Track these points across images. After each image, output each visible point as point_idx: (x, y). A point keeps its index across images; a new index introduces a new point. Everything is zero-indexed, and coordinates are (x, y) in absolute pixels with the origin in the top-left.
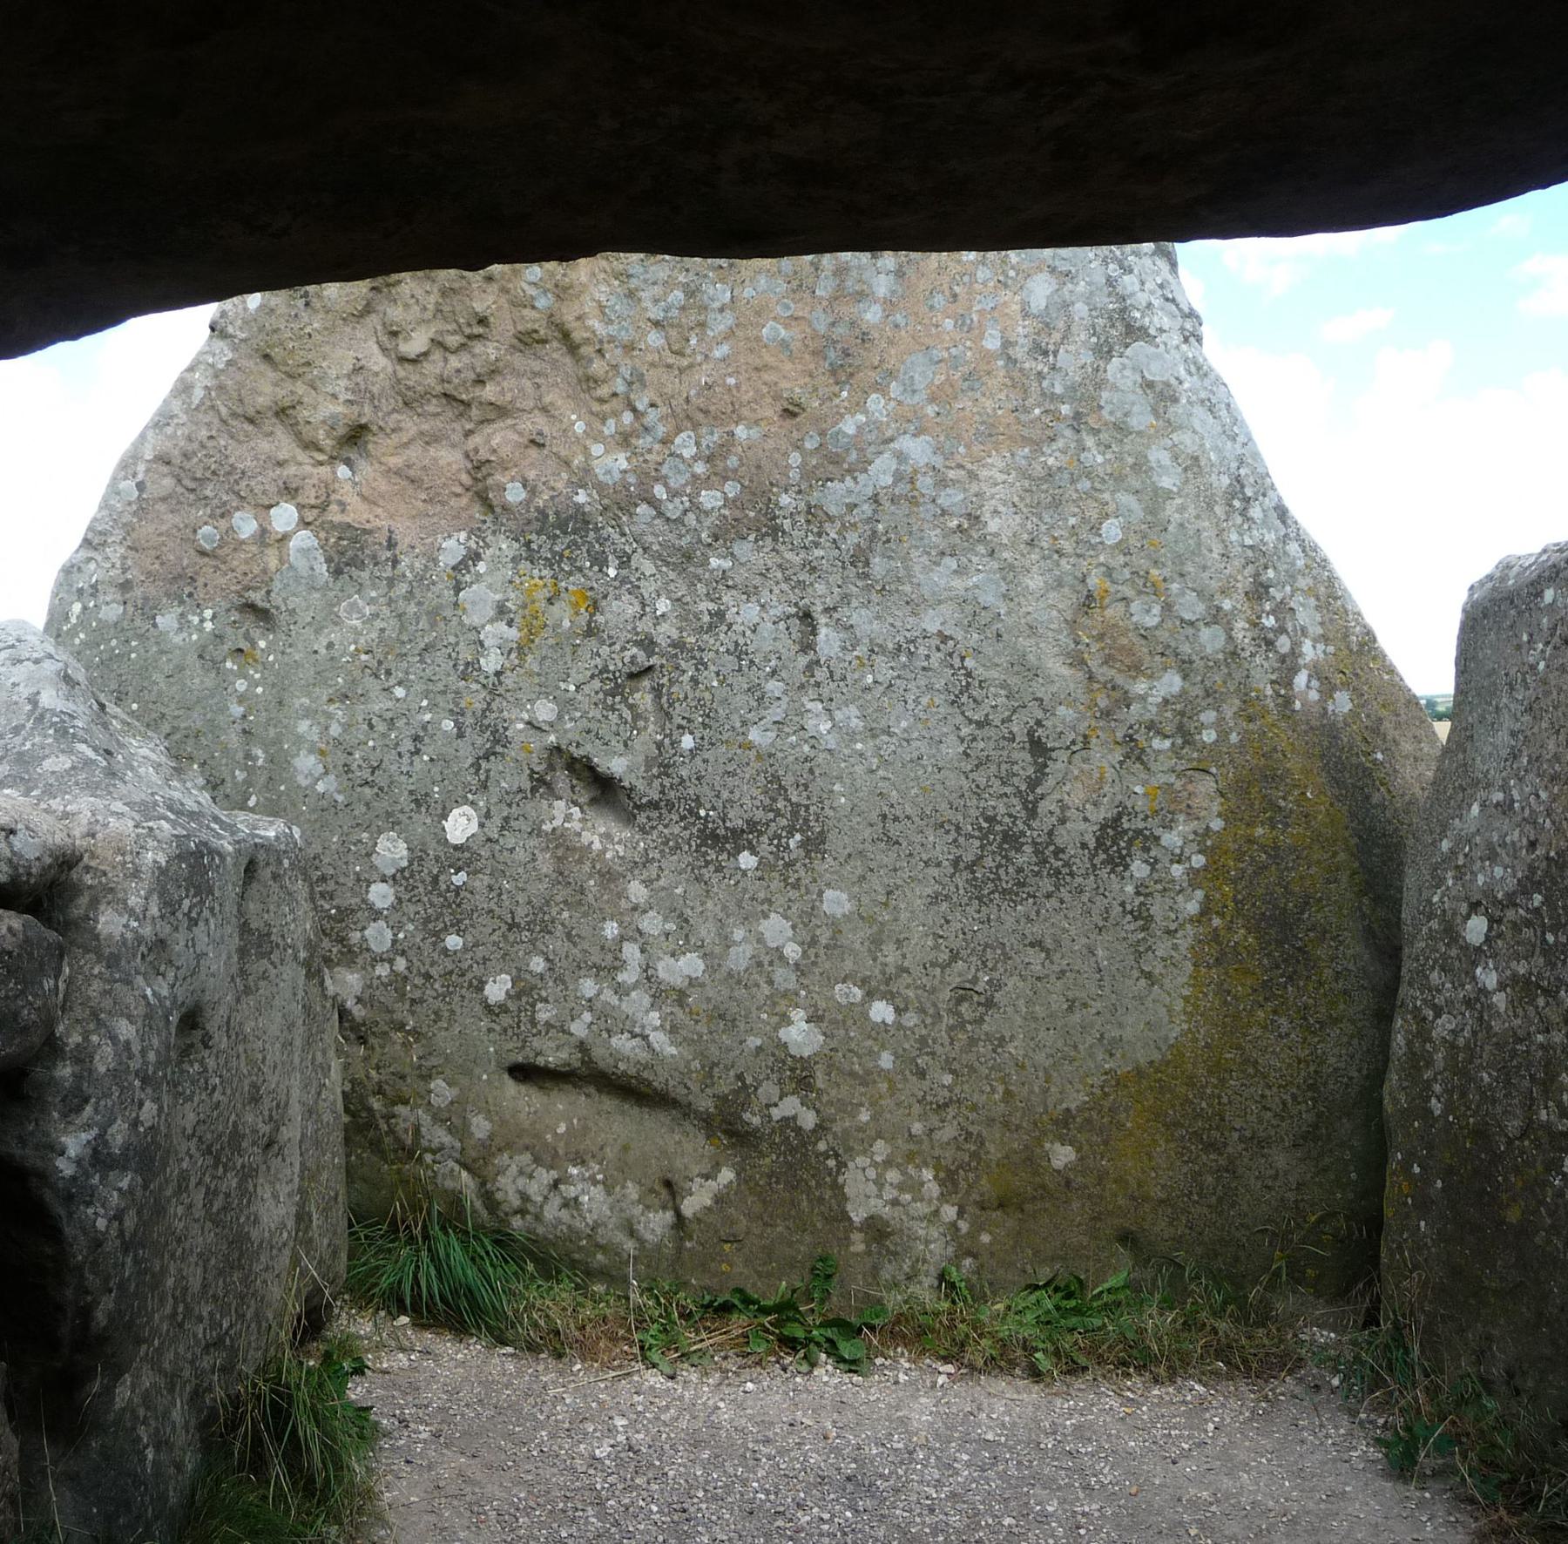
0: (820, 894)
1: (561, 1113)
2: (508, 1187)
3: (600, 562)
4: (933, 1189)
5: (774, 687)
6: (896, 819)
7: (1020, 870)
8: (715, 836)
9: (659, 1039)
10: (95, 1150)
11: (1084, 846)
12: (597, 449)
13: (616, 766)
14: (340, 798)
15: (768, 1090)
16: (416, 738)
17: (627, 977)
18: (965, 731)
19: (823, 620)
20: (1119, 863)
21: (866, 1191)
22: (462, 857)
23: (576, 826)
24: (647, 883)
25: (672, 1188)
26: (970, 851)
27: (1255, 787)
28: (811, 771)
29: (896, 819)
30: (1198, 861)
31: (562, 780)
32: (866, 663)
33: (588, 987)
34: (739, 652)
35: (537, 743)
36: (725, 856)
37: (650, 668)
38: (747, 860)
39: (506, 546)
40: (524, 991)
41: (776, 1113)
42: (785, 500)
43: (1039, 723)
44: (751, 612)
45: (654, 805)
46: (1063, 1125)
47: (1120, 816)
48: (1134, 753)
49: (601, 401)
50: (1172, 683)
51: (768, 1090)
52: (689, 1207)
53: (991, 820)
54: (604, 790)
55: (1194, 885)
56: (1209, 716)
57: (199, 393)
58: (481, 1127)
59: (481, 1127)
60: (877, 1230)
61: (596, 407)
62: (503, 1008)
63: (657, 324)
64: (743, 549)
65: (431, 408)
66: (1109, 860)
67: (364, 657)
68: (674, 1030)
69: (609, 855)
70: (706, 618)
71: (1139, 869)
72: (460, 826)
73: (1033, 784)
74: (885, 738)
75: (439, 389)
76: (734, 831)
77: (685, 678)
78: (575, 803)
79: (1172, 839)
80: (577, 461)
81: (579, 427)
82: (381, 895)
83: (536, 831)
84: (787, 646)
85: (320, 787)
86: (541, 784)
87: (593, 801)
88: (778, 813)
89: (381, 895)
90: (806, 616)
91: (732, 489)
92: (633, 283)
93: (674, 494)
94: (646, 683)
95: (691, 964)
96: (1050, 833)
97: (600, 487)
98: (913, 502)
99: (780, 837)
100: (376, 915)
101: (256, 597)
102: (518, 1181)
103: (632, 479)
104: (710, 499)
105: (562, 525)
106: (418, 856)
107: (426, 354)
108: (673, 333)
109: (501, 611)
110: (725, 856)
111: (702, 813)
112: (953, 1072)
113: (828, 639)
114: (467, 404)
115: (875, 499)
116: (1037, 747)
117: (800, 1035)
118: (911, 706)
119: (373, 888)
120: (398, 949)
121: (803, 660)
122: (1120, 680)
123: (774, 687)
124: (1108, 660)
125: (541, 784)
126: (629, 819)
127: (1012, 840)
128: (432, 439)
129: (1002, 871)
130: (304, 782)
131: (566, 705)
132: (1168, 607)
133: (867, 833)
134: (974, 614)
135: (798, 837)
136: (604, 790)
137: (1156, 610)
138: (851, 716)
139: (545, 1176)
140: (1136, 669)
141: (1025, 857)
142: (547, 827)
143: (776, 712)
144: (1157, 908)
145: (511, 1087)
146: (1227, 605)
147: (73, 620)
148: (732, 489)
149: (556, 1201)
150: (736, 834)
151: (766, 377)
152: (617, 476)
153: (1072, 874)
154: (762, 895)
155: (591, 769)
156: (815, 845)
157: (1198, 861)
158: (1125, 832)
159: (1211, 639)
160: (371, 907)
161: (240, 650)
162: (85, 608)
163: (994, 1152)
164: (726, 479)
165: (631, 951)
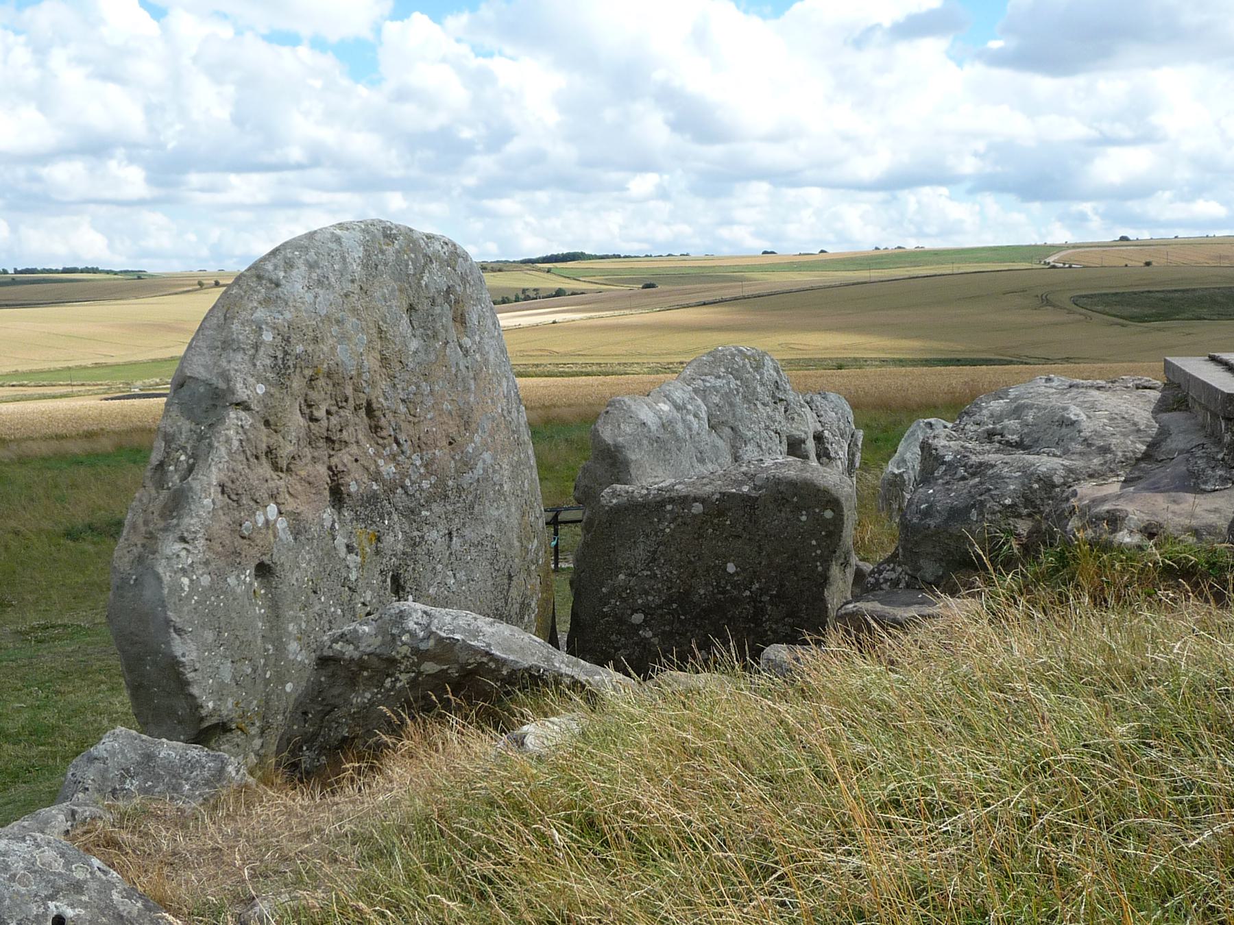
3: (382, 518)
12: (381, 462)
16: (330, 622)
19: (455, 534)
32: (468, 552)
42: (450, 483)
49: (383, 438)
61: (381, 441)
63: (403, 401)
64: (434, 506)
77: (410, 569)
80: (372, 468)
81: (371, 451)
85: (299, 659)
91: (433, 479)
92: (396, 381)
93: (413, 483)
104: (425, 484)
105: (369, 501)
108: (411, 406)
115: (478, 480)
130: (291, 657)
147: (187, 589)
151: (445, 427)
162: (191, 581)
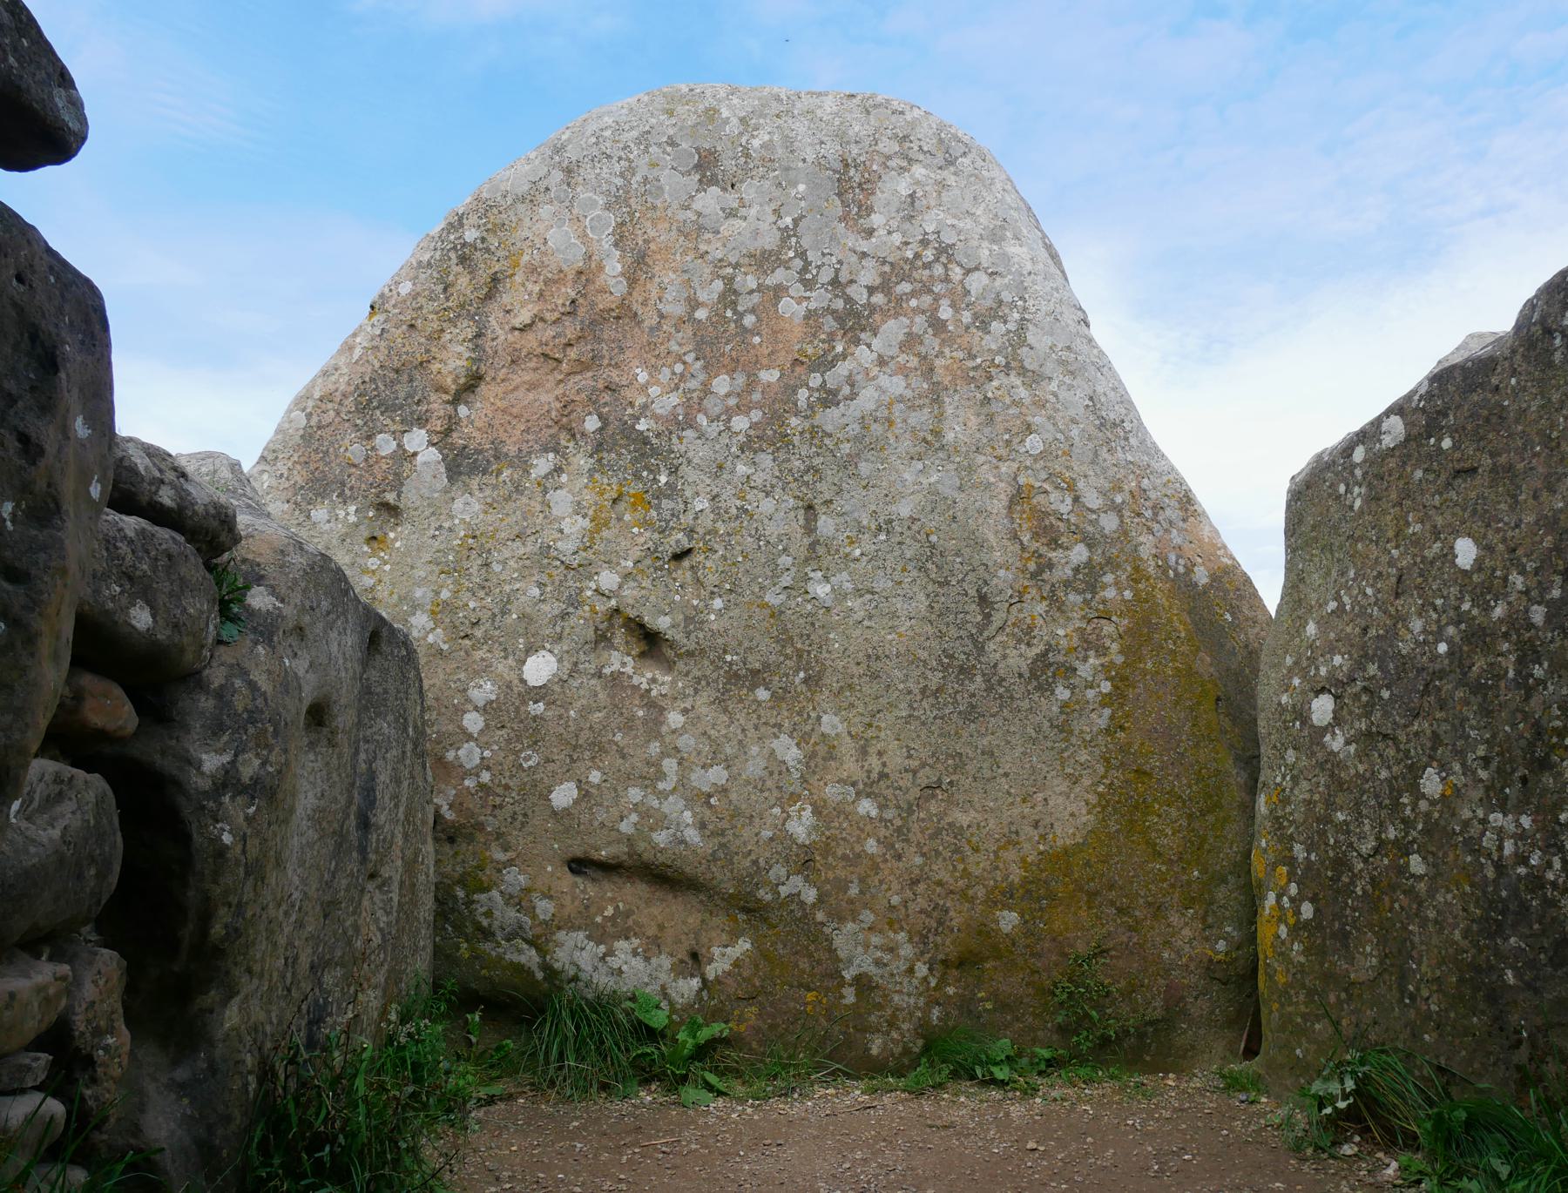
0: (819, 718)
2: (561, 958)
4: (907, 951)
5: (785, 560)
6: (878, 658)
7: (973, 695)
8: (736, 675)
9: (692, 835)
10: (227, 772)
11: (1021, 676)
13: (662, 623)
14: (445, 647)
15: (778, 871)
18: (930, 588)
20: (1046, 689)
22: (539, 693)
23: (629, 670)
24: (685, 711)
25: (696, 959)
26: (935, 679)
27: (1142, 631)
28: (813, 624)
29: (878, 658)
30: (1106, 687)
31: (619, 636)
33: (635, 794)
35: (602, 607)
36: (745, 691)
37: (689, 551)
38: (762, 694)
39: (582, 462)
41: (784, 891)
43: (986, 583)
45: (690, 654)
47: (1047, 651)
50: (1079, 554)
51: (778, 871)
52: (711, 971)
53: (951, 657)
54: (650, 642)
55: (1103, 705)
56: (1109, 578)
57: (358, 352)
58: (545, 908)
59: (545, 908)
60: (863, 984)
62: (567, 812)
65: (532, 365)
66: (1039, 688)
67: (470, 541)
68: (702, 826)
69: (654, 693)
70: (734, 511)
71: (1063, 693)
72: (540, 669)
73: (982, 628)
74: (869, 596)
75: (539, 351)
76: (751, 671)
78: (629, 654)
79: (1085, 671)
82: (473, 722)
83: (599, 675)
84: (796, 528)
85: (431, 639)
86: (602, 639)
87: (642, 655)
88: (787, 657)
89: (473, 722)
90: (810, 507)
91: (756, 415)
94: (686, 563)
95: (718, 775)
96: (995, 666)
97: (656, 417)
98: (890, 422)
99: (787, 675)
100: (469, 737)
101: (390, 497)
103: (680, 410)
107: (530, 325)
110: (745, 691)
111: (728, 658)
112: (923, 855)
113: (826, 525)
114: (558, 361)
116: (983, 600)
117: (801, 826)
118: (889, 571)
119: (467, 716)
120: (485, 765)
121: (807, 541)
122: (1043, 550)
124: (1036, 536)
125: (602, 639)
126: (669, 666)
127: (965, 672)
128: (532, 386)
129: (959, 697)
132: (1076, 499)
133: (856, 670)
134: (935, 500)
135: (802, 675)
136: (650, 642)
137: (1069, 501)
138: (843, 579)
140: (1054, 543)
142: (607, 671)
143: (786, 580)
144: (1077, 725)
146: (1119, 499)
148: (756, 415)
149: (603, 969)
150: (755, 673)
152: (669, 408)
153: (1012, 698)
154: (773, 721)
155: (642, 626)
156: (813, 682)
157: (1106, 687)
158: (1051, 665)
159: (1109, 523)
160: (464, 731)
161: (374, 538)
163: (956, 920)
164: (750, 409)
165: (670, 765)
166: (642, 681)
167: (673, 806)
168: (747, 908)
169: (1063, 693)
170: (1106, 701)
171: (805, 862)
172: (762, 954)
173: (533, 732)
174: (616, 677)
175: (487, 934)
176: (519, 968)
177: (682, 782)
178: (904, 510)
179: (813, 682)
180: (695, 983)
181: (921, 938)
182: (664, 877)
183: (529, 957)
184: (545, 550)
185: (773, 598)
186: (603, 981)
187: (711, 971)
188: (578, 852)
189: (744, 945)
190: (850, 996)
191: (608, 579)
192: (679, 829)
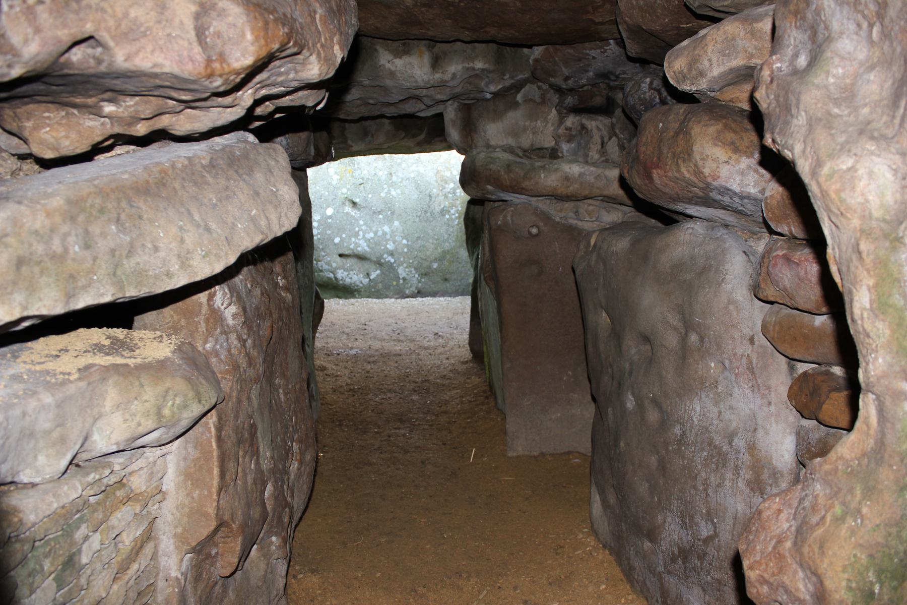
1: (349, 262)
4: (414, 272)
5: (385, 186)
9: (367, 248)
13: (357, 200)
15: (385, 256)
17: (360, 237)
20: (444, 215)
21: (402, 272)
22: (330, 217)
25: (368, 275)
31: (347, 203)
33: (353, 239)
34: (379, 180)
38: (381, 216)
40: (342, 240)
44: (381, 173)
46: (436, 260)
48: (446, 196)
52: (372, 277)
58: (334, 265)
59: (334, 265)
60: (404, 279)
68: (368, 246)
71: (447, 216)
72: (330, 212)
79: (452, 211)
86: (344, 204)
95: (372, 235)
102: (340, 274)
106: (322, 217)
109: (336, 173)
113: (394, 178)
116: (430, 196)
117: (390, 246)
123: (385, 186)
126: (359, 210)
131: (348, 189)
136: (354, 204)
138: (399, 191)
139: (346, 273)
140: (446, 183)
141: (429, 214)
145: (339, 259)
165: (361, 233)
166: (353, 214)
167: (361, 242)
168: (379, 264)
169: (447, 216)
170: (456, 218)
171: (391, 254)
172: (382, 273)
173: (329, 227)
174: (347, 213)
175: (321, 271)
176: (330, 279)
177: (364, 236)
178: (412, 175)
179: (393, 213)
180: (367, 280)
181: (416, 269)
182: (361, 258)
183: (331, 275)
184: (330, 184)
185: (383, 195)
186: (348, 281)
187: (372, 277)
188: (341, 252)
189: (378, 272)
190: (401, 281)
191: (344, 190)
192: (363, 247)
